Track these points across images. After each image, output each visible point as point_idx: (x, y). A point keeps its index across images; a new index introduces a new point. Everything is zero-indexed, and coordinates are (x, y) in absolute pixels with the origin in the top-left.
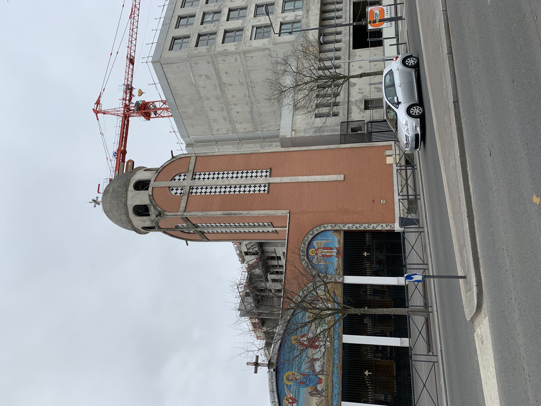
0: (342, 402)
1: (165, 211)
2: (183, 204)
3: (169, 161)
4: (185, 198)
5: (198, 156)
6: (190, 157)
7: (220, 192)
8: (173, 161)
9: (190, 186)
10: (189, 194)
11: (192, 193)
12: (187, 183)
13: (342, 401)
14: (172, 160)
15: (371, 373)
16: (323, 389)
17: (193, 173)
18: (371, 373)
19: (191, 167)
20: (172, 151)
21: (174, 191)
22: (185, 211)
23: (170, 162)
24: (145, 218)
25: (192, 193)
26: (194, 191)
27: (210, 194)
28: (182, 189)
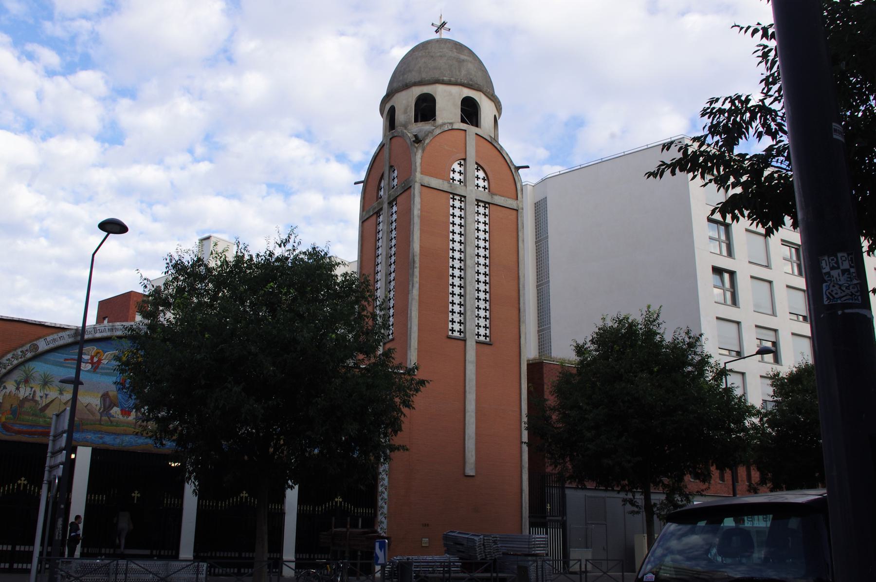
0: (91, 448)
1: (423, 151)
2: (435, 182)
3: (511, 162)
4: (445, 186)
5: (517, 215)
7: (454, 216)
8: (510, 168)
9: (465, 197)
10: (451, 193)
11: (454, 199)
12: (472, 191)
13: (92, 449)
14: (512, 167)
15: (135, 502)
16: (113, 416)
17: (489, 203)
18: (135, 502)
19: (498, 200)
20: (527, 167)
21: (457, 168)
22: (422, 185)
23: (509, 162)
25: (454, 199)
26: (457, 204)
27: (451, 206)
28: (460, 181)
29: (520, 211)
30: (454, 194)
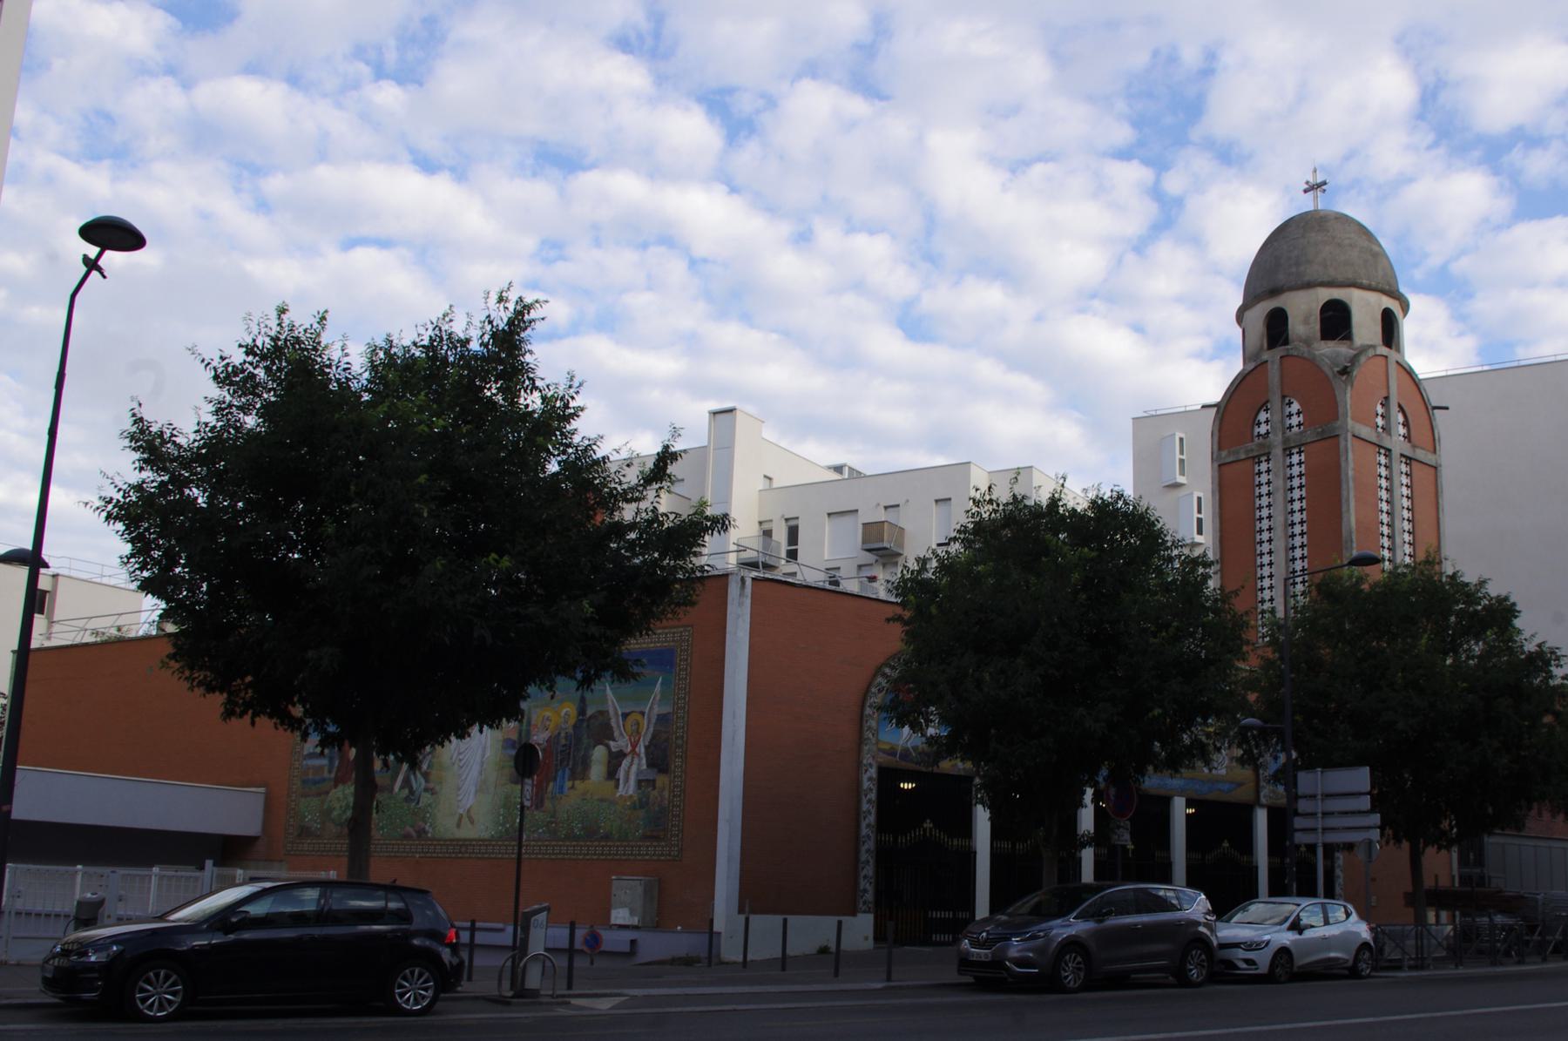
1: (1352, 386)
2: (1365, 432)
3: (1429, 400)
6: (1432, 450)
9: (1390, 450)
11: (1291, 427)
14: (1429, 407)
17: (1410, 459)
19: (1420, 454)
20: (1447, 408)
21: (1380, 410)
22: (1354, 436)
23: (1426, 401)
24: (1316, 326)
25: (1291, 427)
26: (1383, 460)
29: (1439, 469)
30: (1380, 447)
